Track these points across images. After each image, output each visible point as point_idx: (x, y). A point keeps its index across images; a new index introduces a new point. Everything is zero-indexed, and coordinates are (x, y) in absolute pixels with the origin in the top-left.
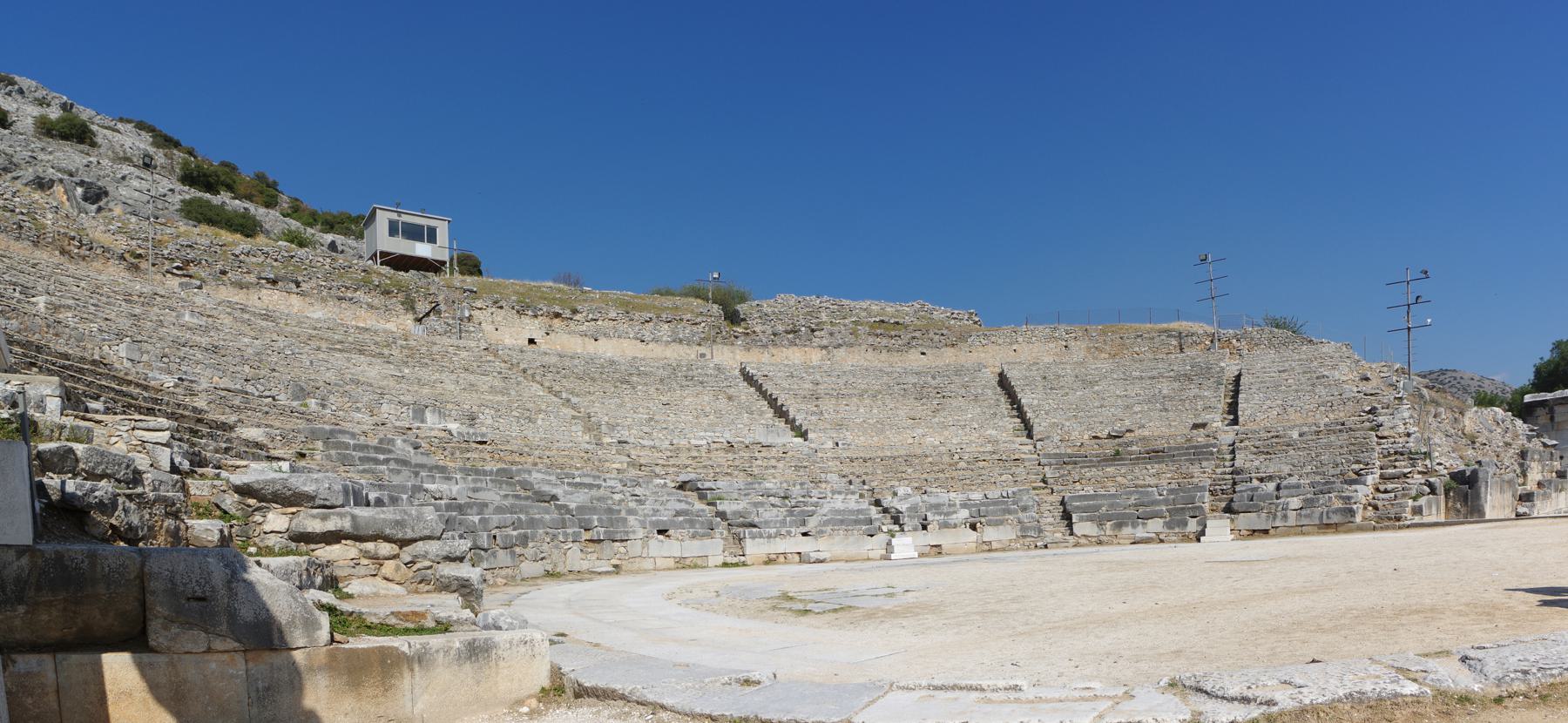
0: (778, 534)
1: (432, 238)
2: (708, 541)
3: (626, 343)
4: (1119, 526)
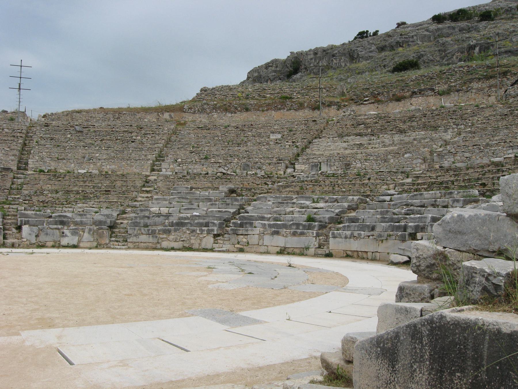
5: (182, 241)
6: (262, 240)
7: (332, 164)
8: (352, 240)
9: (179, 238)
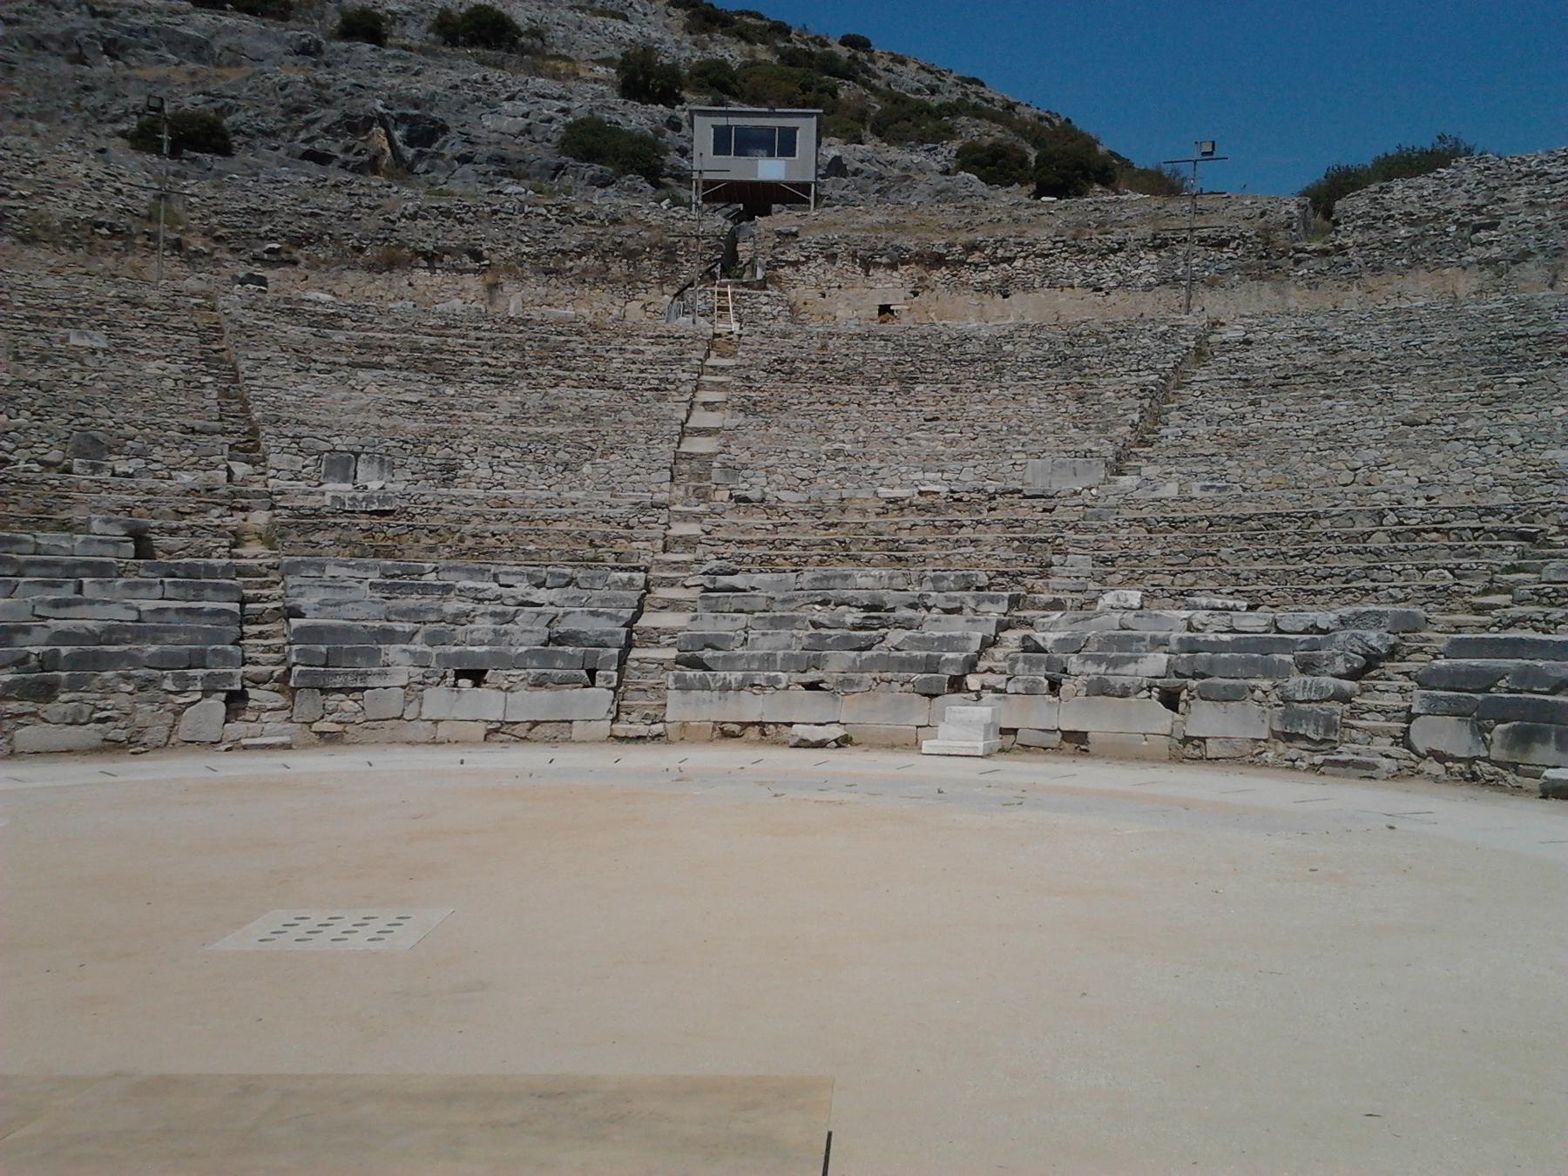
0: (747, 684)
1: (788, 149)
2: (574, 694)
3: (1062, 298)
4: (1524, 738)
5: (99, 720)
6: (416, 702)
7: (397, 462)
8: (745, 694)
9: (87, 709)
